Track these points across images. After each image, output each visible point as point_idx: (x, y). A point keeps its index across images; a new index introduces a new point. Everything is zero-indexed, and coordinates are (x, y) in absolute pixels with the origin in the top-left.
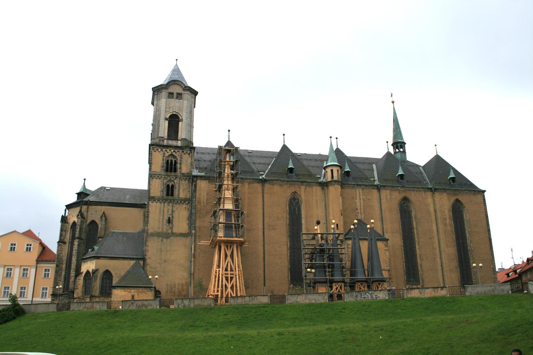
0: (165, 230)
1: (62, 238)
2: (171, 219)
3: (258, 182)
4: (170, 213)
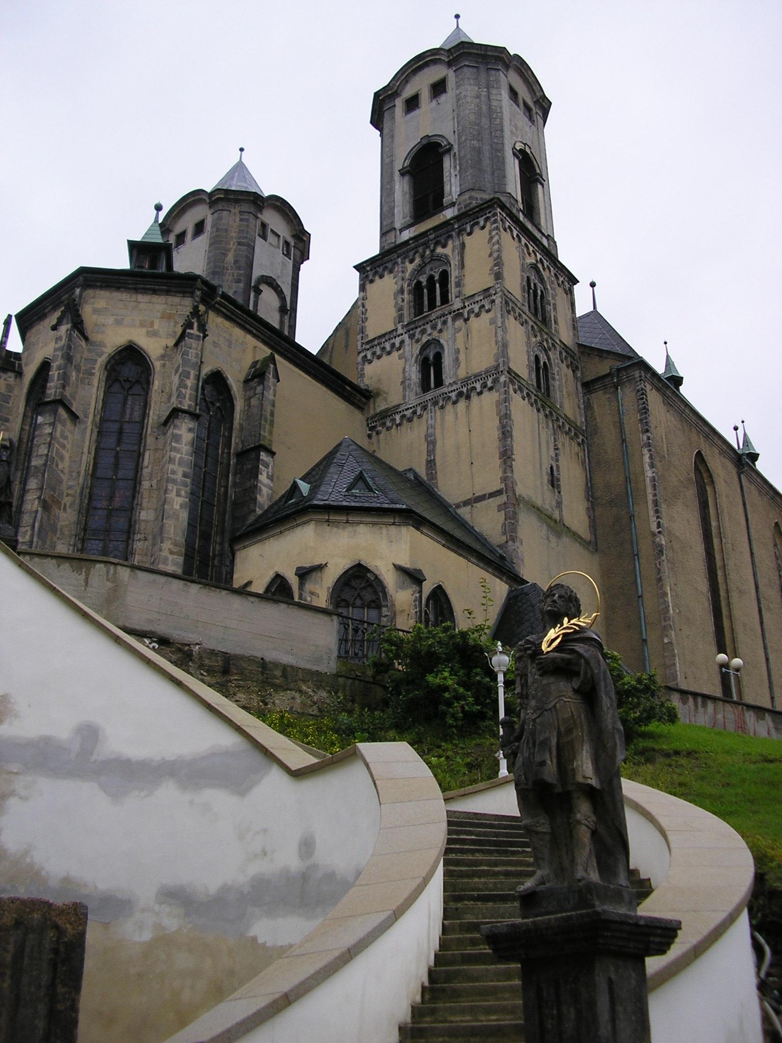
0: (547, 507)
1: (68, 392)
2: (555, 473)
3: (731, 459)
4: (552, 453)
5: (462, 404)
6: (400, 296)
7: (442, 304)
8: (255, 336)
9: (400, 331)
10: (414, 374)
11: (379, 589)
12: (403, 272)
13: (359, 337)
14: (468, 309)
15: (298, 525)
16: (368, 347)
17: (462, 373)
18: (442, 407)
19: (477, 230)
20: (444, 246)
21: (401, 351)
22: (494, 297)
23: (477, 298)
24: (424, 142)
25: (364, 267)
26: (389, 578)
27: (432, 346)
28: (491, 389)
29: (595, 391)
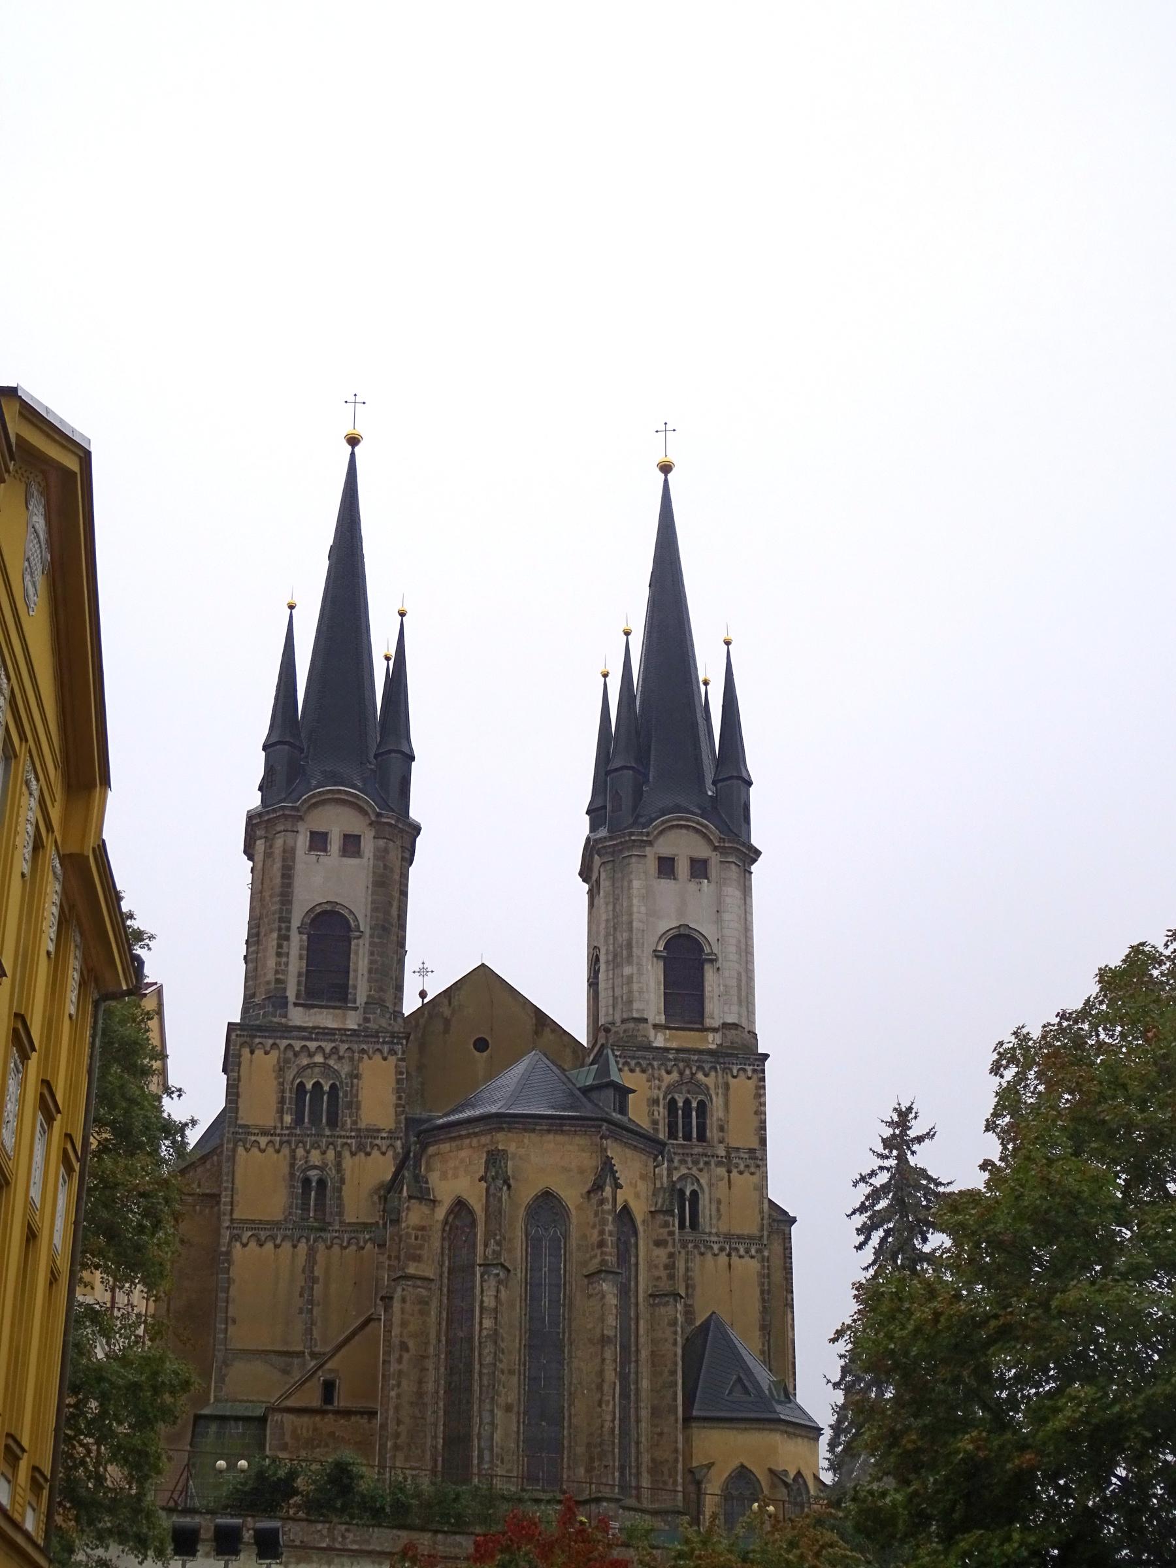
6: (655, 1108)
17: (724, 1229)
20: (706, 1075)
23: (742, 1155)
28: (752, 1257)
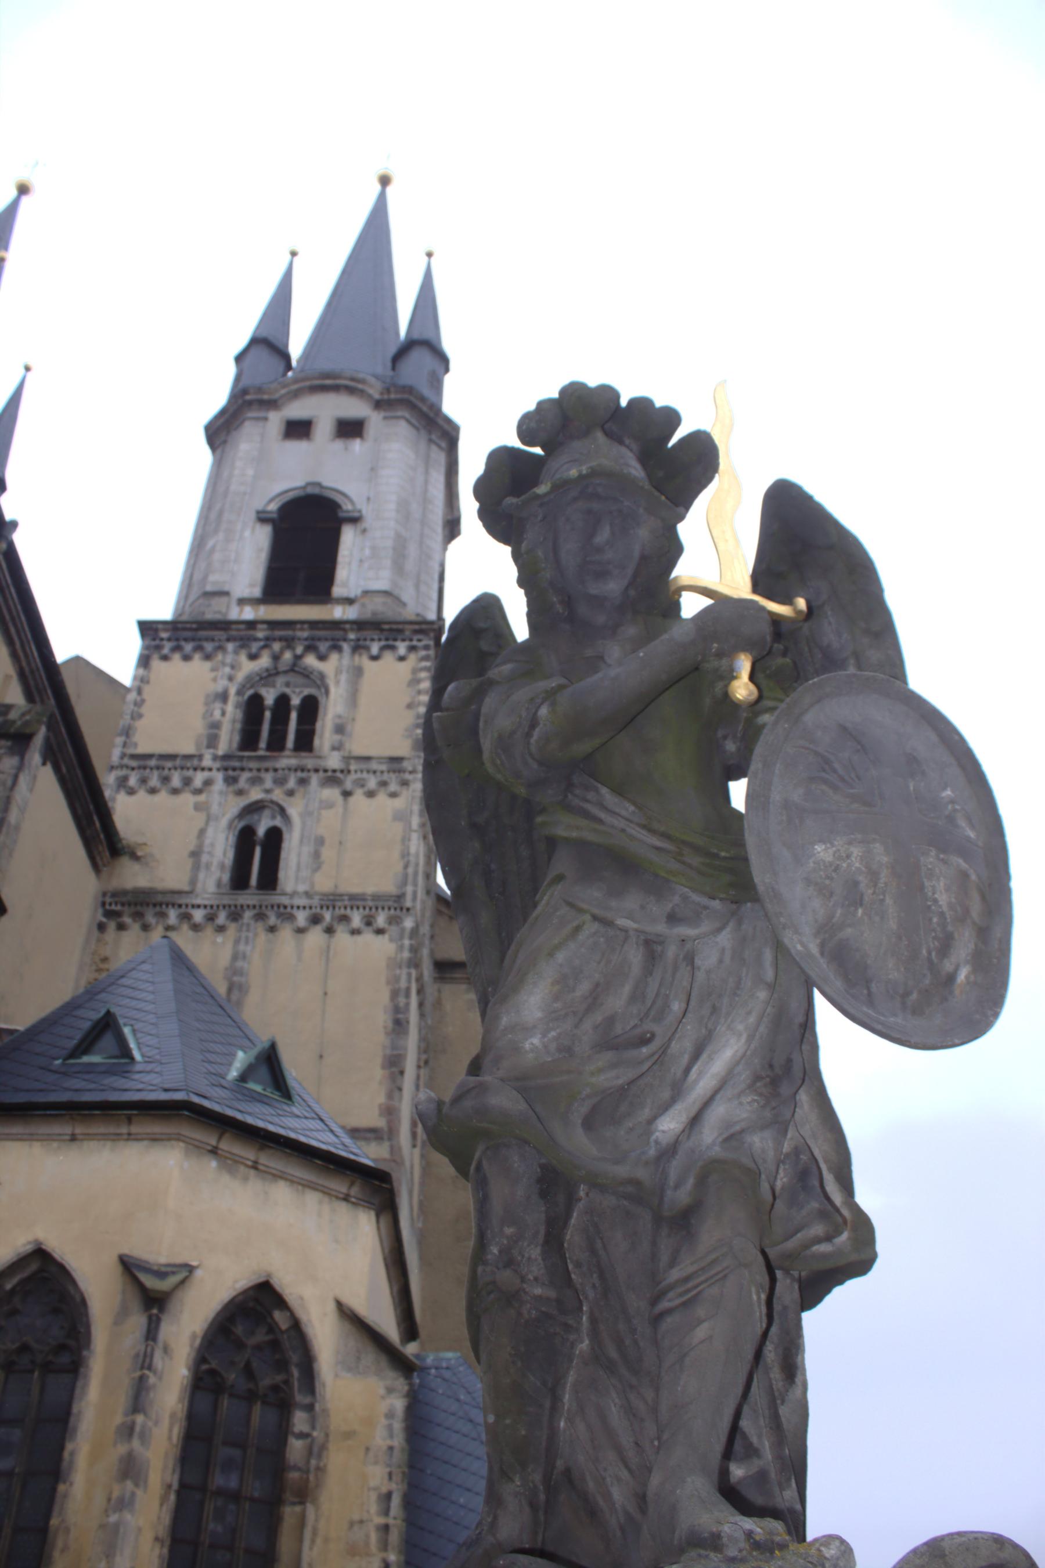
5: (315, 937)
7: (270, 747)
8: (14, 655)
9: (207, 762)
10: (221, 848)
11: (295, 1358)
12: (233, 667)
13: (119, 740)
14: (353, 776)
15: (130, 1137)
16: (134, 763)
17: (324, 883)
18: (272, 929)
19: (388, 657)
20: (322, 658)
21: (202, 798)
22: (407, 776)
23: (374, 765)
24: (310, 490)
25: (156, 630)
26: (325, 1336)
27: (267, 813)
28: (380, 932)
29: (453, 980)
